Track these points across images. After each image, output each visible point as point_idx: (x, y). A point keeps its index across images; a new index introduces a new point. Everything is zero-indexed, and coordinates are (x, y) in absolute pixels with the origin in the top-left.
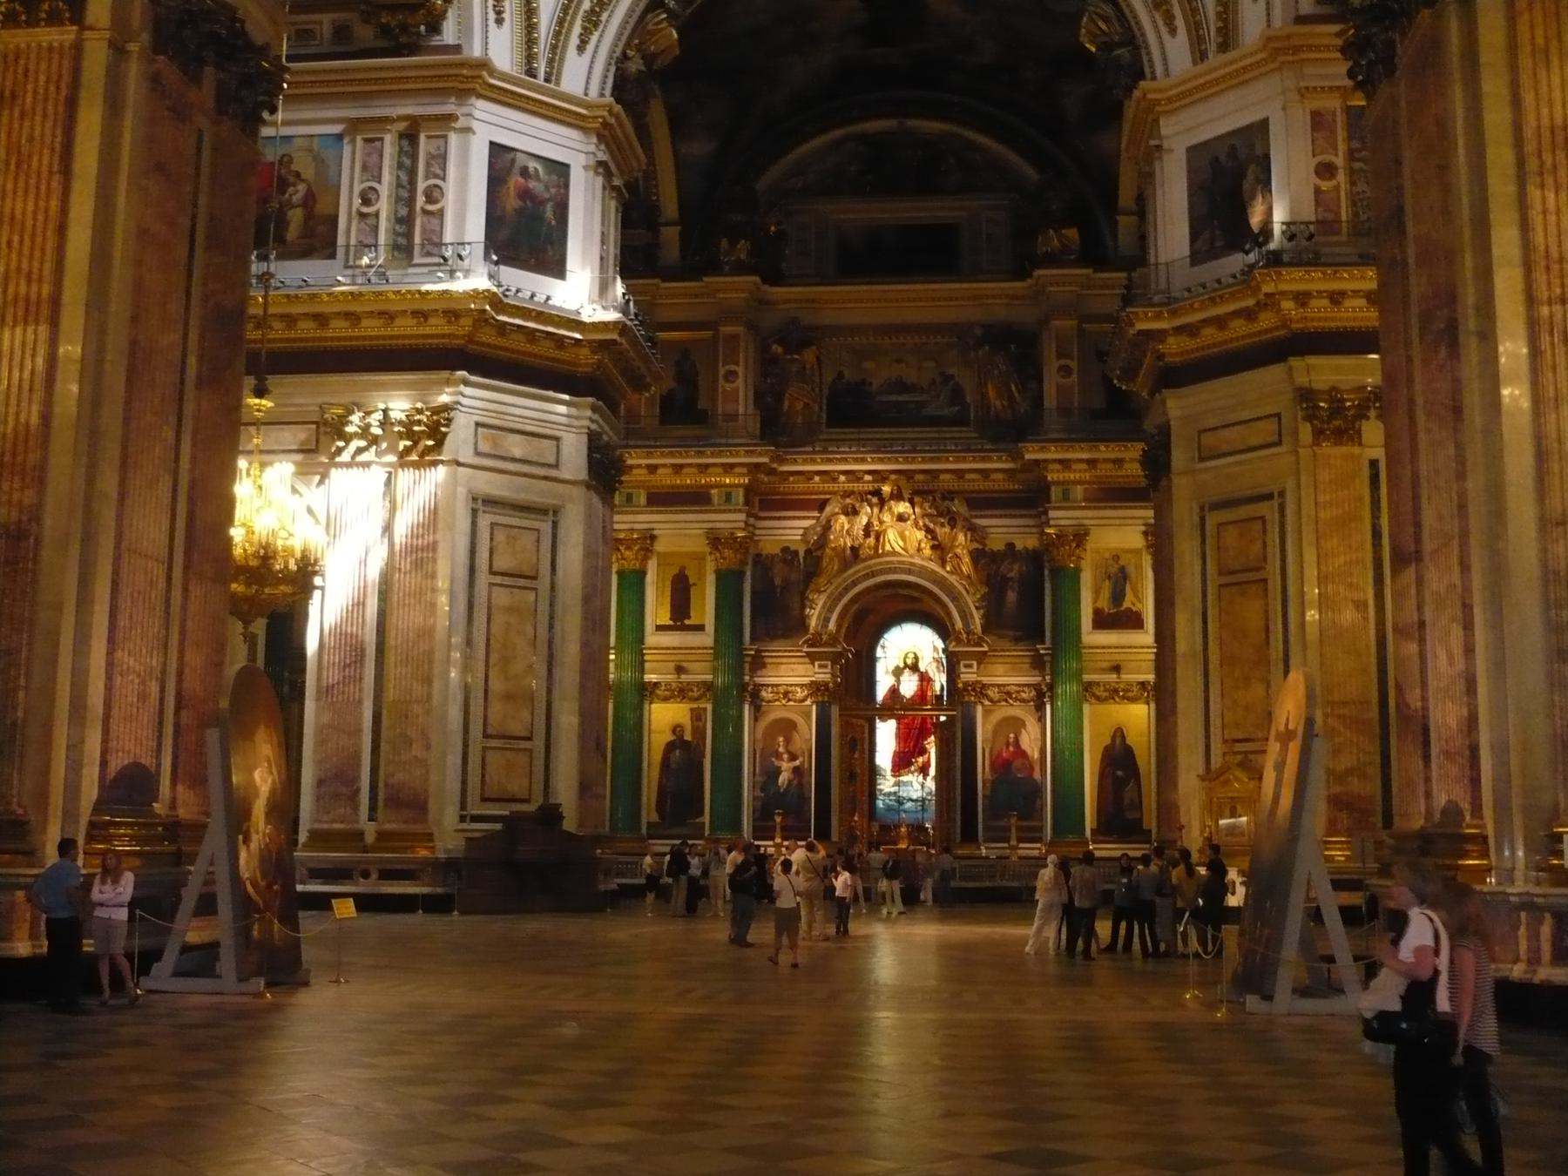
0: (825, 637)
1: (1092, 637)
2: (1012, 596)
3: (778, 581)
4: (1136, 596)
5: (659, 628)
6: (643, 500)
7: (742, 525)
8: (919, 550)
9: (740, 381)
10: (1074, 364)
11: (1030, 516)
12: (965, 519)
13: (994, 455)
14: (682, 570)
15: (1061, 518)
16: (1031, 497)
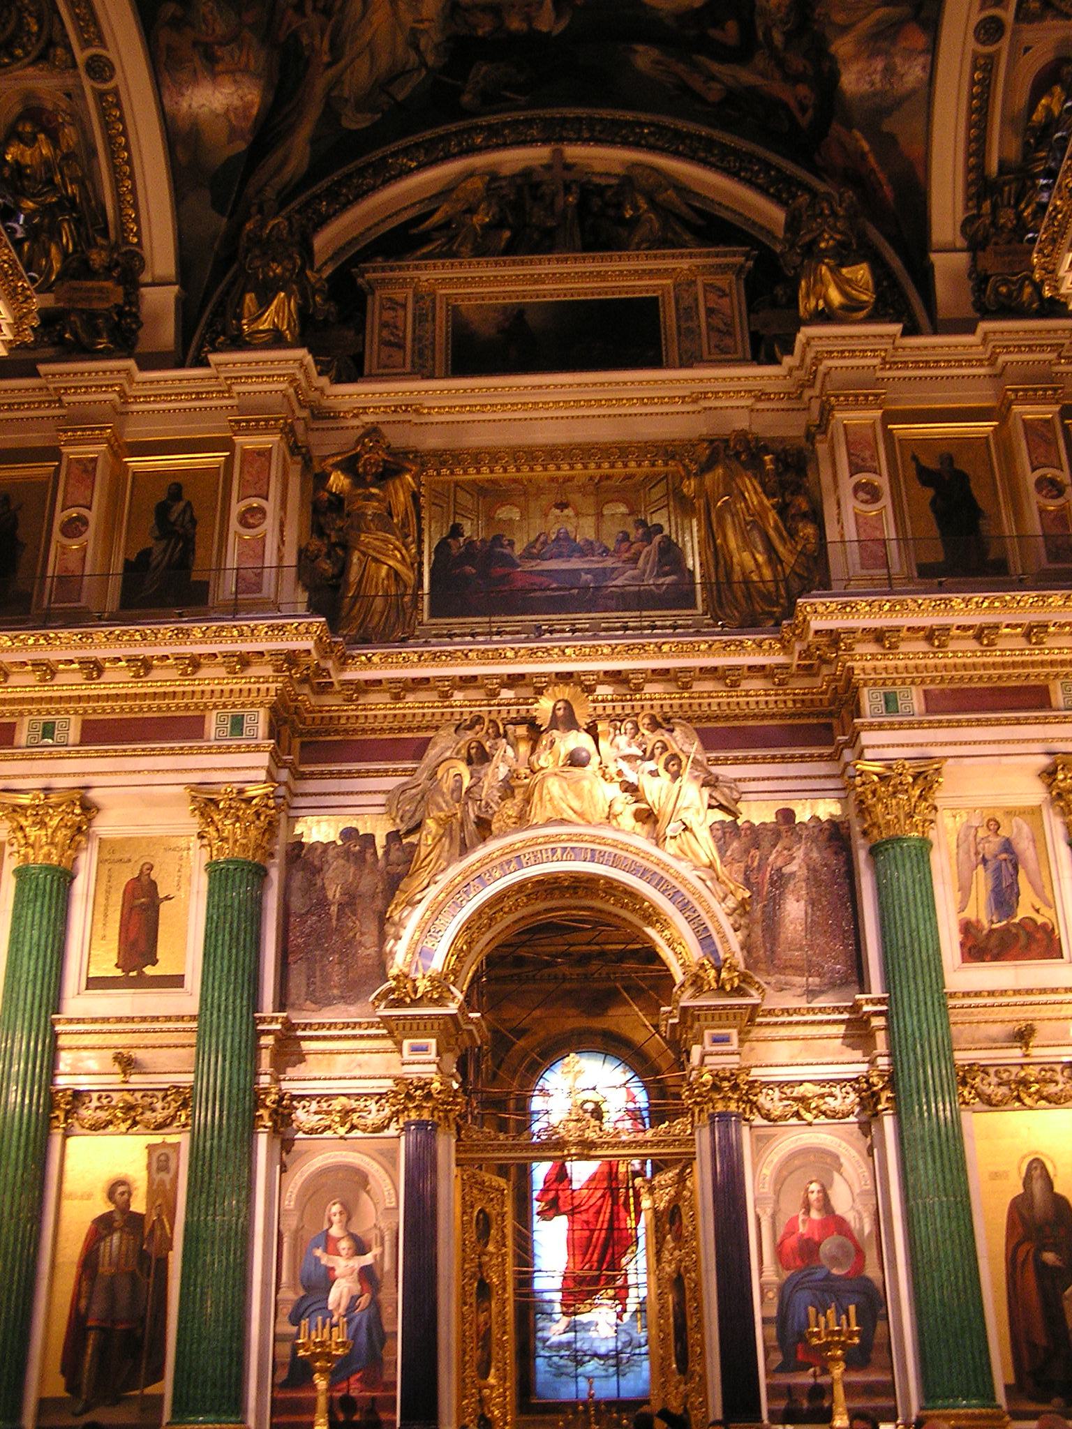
0: (423, 985)
1: (962, 976)
2: (794, 909)
3: (334, 892)
4: (1039, 893)
5: (94, 983)
6: (74, 734)
7: (262, 775)
8: (611, 816)
9: (269, 526)
10: (883, 482)
11: (821, 757)
12: (695, 761)
13: (748, 640)
14: (151, 868)
15: (882, 746)
16: (820, 723)
